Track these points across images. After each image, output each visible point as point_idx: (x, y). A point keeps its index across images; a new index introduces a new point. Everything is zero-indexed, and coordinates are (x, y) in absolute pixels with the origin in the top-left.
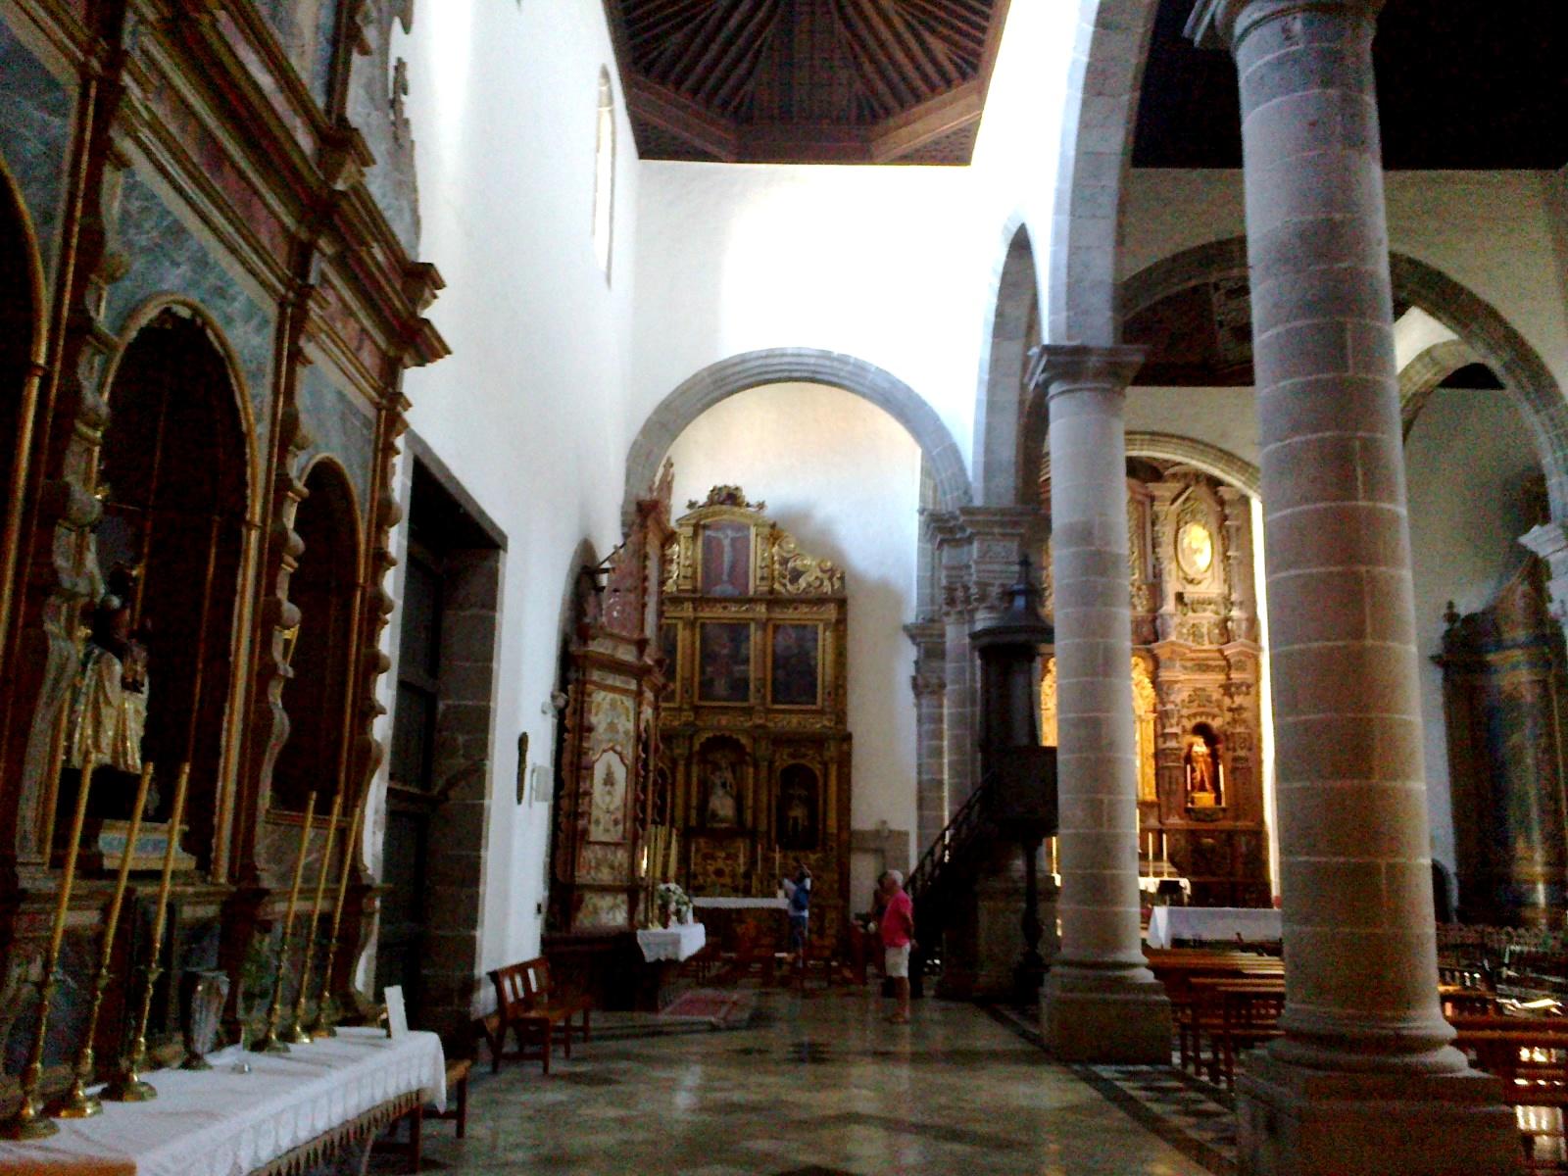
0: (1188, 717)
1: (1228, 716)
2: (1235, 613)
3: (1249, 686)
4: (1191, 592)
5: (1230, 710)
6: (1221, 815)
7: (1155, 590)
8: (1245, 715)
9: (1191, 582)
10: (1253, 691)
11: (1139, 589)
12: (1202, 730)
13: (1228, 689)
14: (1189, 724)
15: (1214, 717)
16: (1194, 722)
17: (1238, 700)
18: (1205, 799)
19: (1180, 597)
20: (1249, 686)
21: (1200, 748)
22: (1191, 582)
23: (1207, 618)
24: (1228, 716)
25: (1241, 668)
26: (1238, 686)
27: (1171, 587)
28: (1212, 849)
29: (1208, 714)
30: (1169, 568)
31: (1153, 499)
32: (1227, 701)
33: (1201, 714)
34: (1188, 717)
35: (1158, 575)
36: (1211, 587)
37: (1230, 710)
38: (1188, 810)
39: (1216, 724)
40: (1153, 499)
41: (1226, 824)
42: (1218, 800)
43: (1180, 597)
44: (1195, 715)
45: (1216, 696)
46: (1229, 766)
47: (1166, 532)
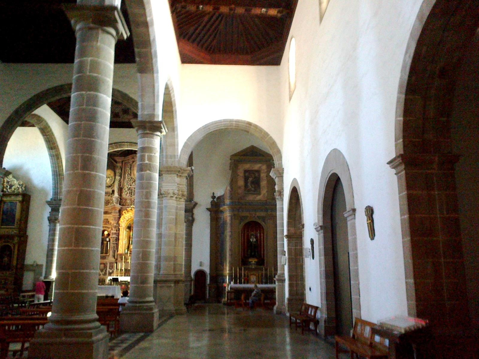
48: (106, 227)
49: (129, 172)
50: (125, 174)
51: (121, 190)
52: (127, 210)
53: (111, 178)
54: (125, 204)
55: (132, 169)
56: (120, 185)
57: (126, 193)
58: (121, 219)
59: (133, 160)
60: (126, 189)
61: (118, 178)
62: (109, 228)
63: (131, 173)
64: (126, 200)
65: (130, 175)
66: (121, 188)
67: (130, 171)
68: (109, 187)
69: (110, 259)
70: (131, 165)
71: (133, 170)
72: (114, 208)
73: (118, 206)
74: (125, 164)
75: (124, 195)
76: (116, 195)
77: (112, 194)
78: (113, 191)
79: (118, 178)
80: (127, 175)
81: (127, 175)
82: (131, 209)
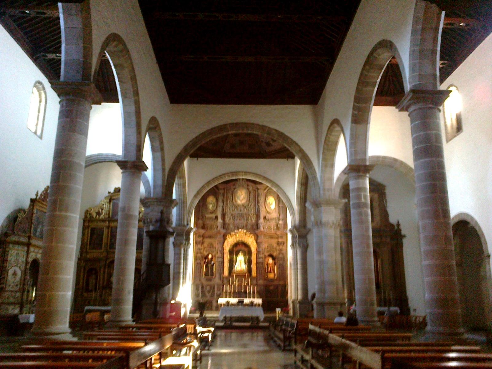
2: (281, 222)
4: (268, 216)
7: (258, 216)
9: (269, 213)
10: (285, 245)
13: (278, 244)
14: (267, 254)
17: (281, 247)
18: (271, 276)
19: (265, 218)
20: (284, 244)
21: (271, 261)
23: (273, 224)
25: (282, 237)
27: (262, 215)
30: (262, 209)
31: (258, 189)
32: (278, 248)
35: (259, 211)
36: (274, 215)
39: (275, 254)
40: (258, 189)
42: (275, 275)
43: (265, 218)
47: (262, 199)
50: (227, 201)
51: (224, 216)
53: (213, 205)
55: (233, 195)
56: (223, 210)
58: (226, 243)
59: (234, 187)
60: (229, 215)
61: (220, 204)
63: (233, 199)
64: (229, 224)
67: (231, 198)
69: (216, 280)
71: (235, 197)
72: (219, 233)
73: (223, 231)
74: (227, 190)
75: (227, 220)
76: (220, 220)
77: (215, 219)
78: (217, 217)
79: (220, 204)
80: (229, 202)
81: (229, 202)
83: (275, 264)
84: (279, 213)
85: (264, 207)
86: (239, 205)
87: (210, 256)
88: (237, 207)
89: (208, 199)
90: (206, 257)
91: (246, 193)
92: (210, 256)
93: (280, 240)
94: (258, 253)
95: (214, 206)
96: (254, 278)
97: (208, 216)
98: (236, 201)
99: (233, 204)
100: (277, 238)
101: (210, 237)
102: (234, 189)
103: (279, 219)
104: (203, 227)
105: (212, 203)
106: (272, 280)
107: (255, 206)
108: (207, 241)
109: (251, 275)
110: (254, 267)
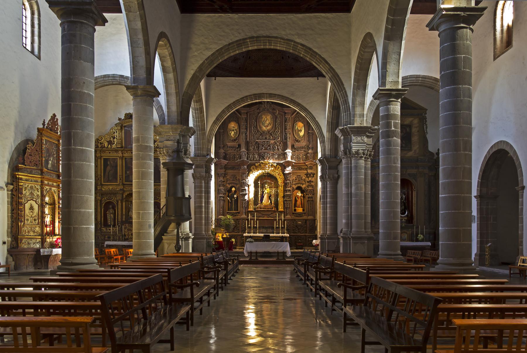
0: (295, 184)
1: (307, 184)
3: (314, 174)
4: (297, 145)
5: (308, 182)
6: (303, 215)
8: (313, 184)
9: (297, 141)
11: (280, 143)
12: (299, 188)
13: (308, 175)
14: (295, 187)
15: (303, 184)
16: (297, 186)
17: (310, 179)
18: (300, 210)
20: (314, 174)
21: (299, 194)
22: (297, 141)
24: (307, 184)
25: (311, 168)
26: (310, 175)
27: (289, 144)
28: (301, 225)
29: (301, 184)
31: (285, 113)
32: (307, 179)
33: (299, 183)
34: (295, 184)
35: (286, 139)
37: (308, 182)
38: (293, 213)
39: (303, 186)
41: (305, 217)
42: (303, 210)
44: (297, 184)
45: (304, 178)
46: (307, 199)
47: (289, 125)
48: (233, 183)
49: (255, 125)
50: (250, 127)
52: (255, 165)
54: (253, 159)
57: (253, 147)
59: (258, 111)
62: (237, 184)
65: (257, 127)
66: (247, 142)
68: (235, 140)
70: (257, 117)
74: (250, 115)
76: (243, 149)
77: (237, 148)
78: (239, 146)
82: (260, 165)
83: (304, 197)
84: (309, 141)
85: (292, 133)
86: (264, 132)
87: (233, 189)
88: (263, 133)
89: (229, 127)
90: (230, 191)
91: (271, 118)
92: (233, 189)
93: (309, 171)
94: (285, 185)
95: (236, 133)
96: (281, 212)
97: (230, 144)
98: (261, 128)
99: (258, 131)
100: (306, 169)
101: (233, 168)
102: (259, 113)
103: (308, 148)
104: (225, 158)
105: (233, 130)
106: (300, 215)
107: (282, 132)
108: (230, 172)
109: (278, 209)
110: (280, 200)
